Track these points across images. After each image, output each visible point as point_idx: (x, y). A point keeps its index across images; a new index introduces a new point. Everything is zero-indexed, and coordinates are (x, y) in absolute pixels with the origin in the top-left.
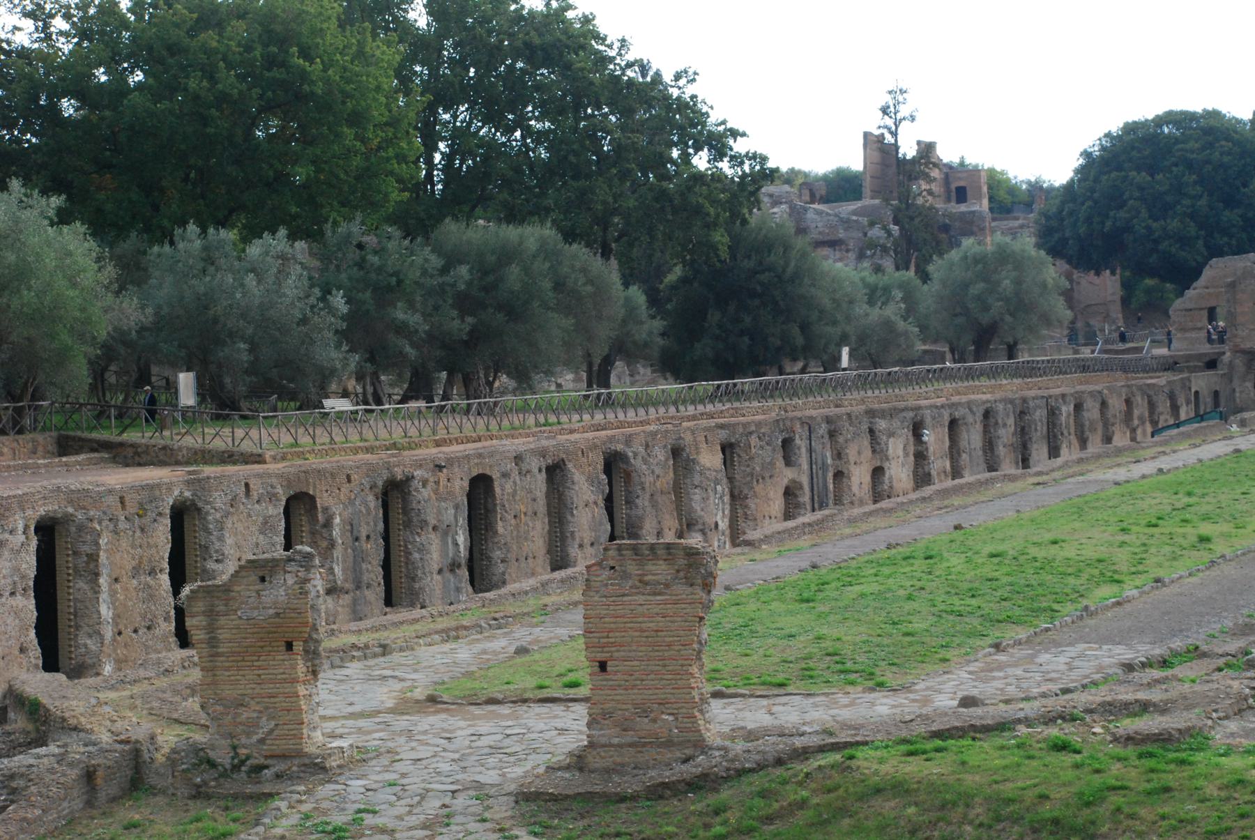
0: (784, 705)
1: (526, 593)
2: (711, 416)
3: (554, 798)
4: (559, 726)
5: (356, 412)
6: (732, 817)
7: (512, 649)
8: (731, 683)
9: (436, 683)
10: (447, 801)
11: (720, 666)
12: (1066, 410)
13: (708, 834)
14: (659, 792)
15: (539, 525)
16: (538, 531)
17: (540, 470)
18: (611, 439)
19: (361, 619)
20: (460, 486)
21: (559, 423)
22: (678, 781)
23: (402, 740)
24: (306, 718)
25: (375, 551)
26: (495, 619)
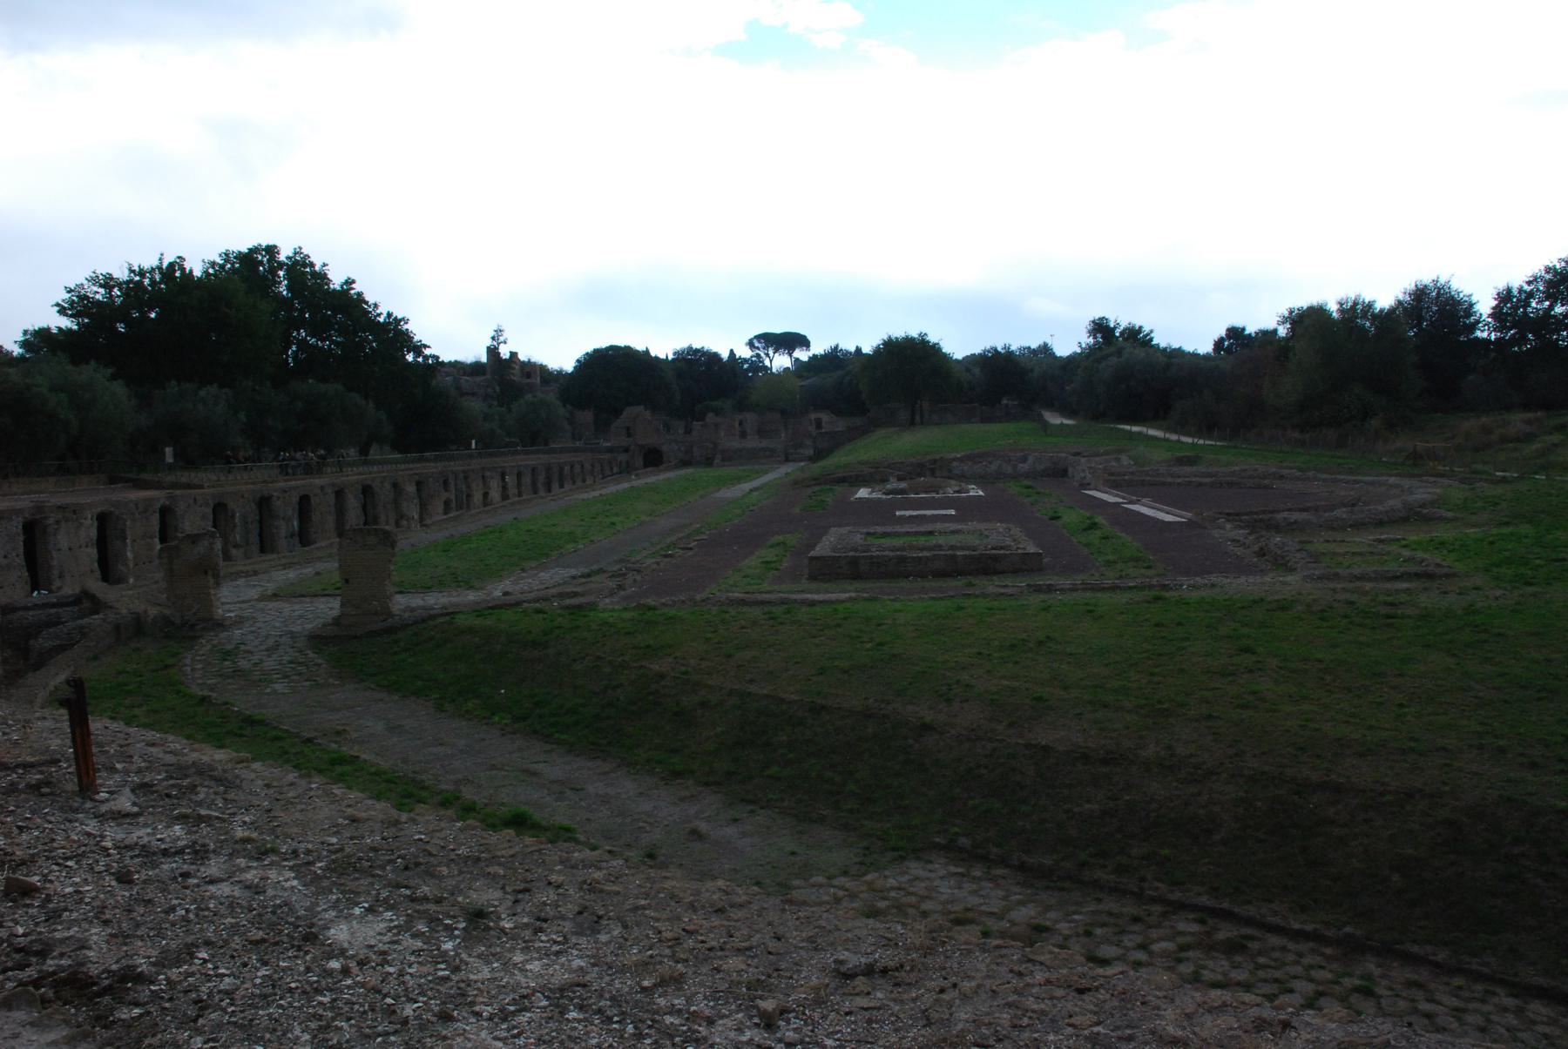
12: (567, 468)
20: (295, 499)
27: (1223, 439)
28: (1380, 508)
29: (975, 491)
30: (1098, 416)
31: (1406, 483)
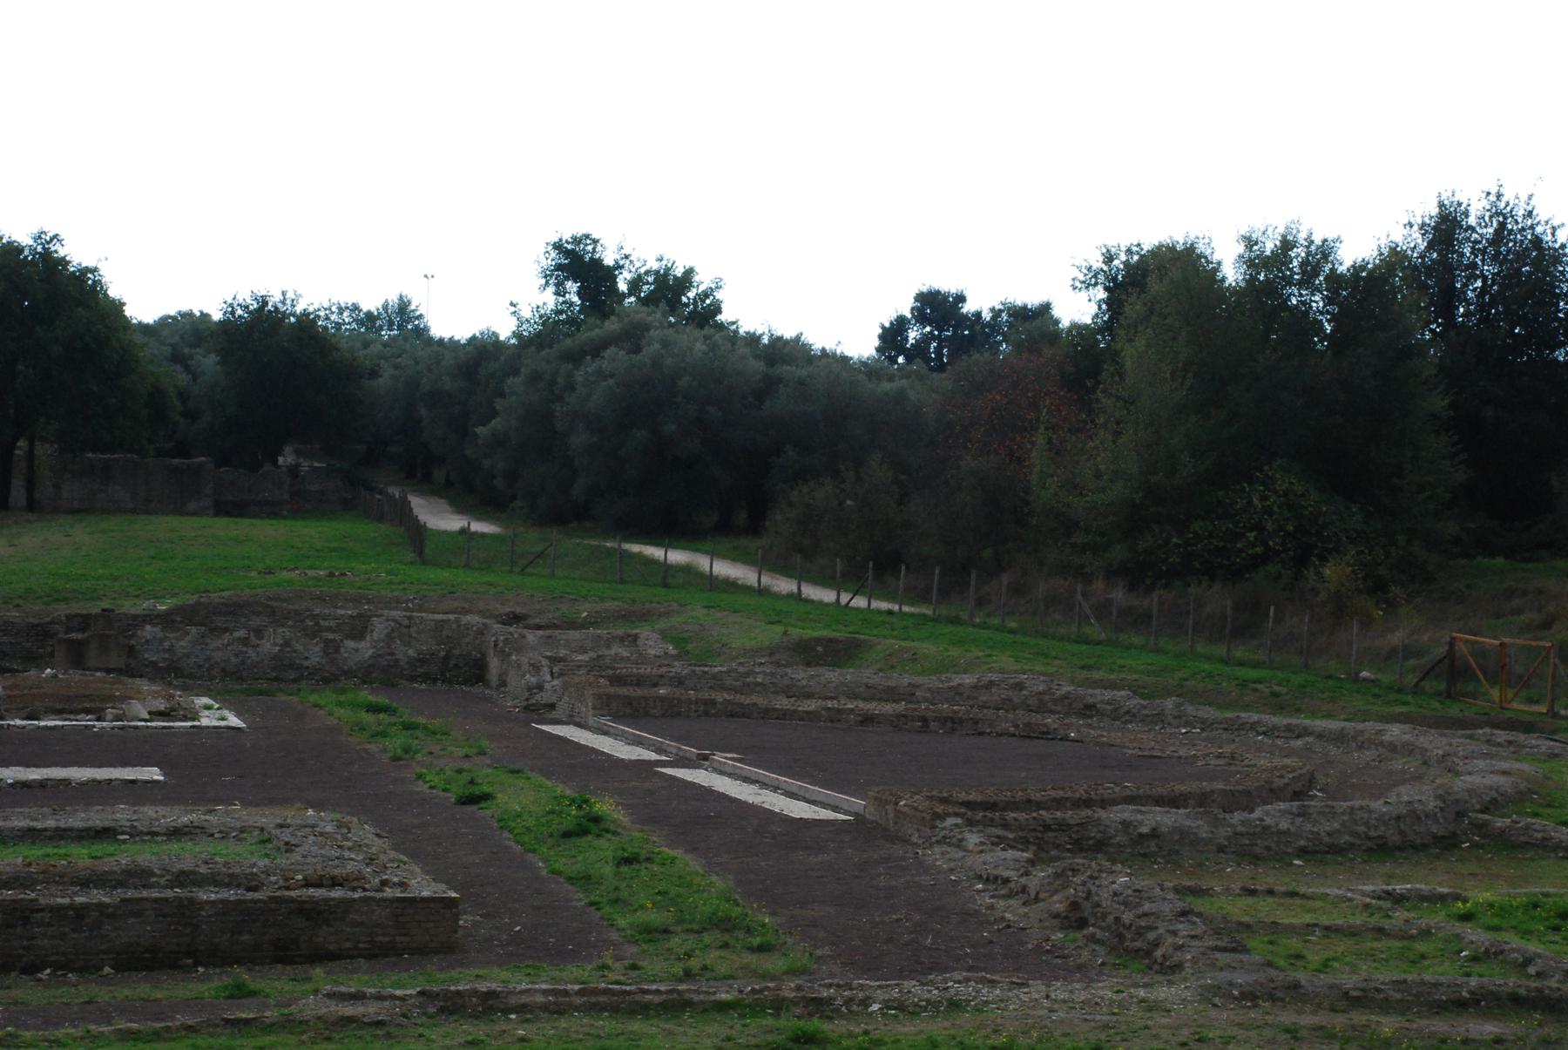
27: (922, 597)
28: (1377, 805)
29: (214, 715)
30: (565, 514)
31: (1434, 742)
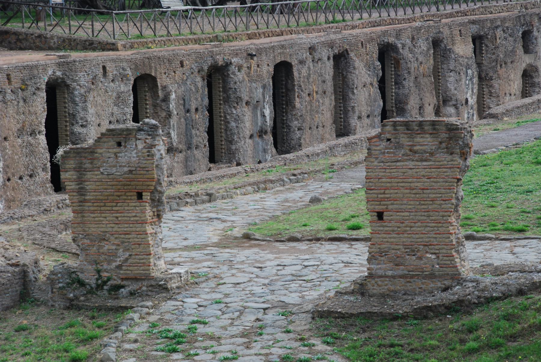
0: (524, 246)
1: (318, 155)
2: (465, 14)
3: (342, 316)
4: (345, 259)
5: (187, 11)
6: (484, 334)
7: (308, 199)
8: (480, 229)
9: (250, 224)
10: (260, 316)
11: (471, 215)
13: (463, 347)
14: (424, 313)
15: (327, 101)
16: (327, 105)
17: (329, 58)
18: (385, 33)
19: (191, 173)
20: (267, 70)
21: (344, 20)
22: (439, 305)
23: (225, 268)
24: (152, 250)
25: (201, 120)
26: (294, 175)
